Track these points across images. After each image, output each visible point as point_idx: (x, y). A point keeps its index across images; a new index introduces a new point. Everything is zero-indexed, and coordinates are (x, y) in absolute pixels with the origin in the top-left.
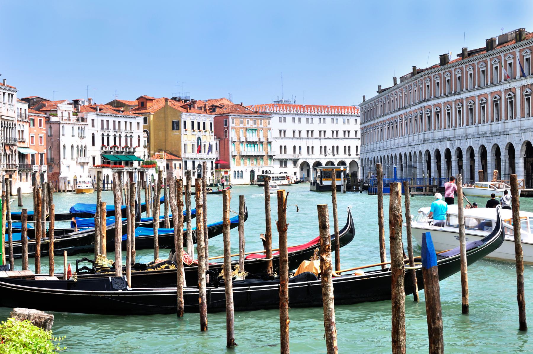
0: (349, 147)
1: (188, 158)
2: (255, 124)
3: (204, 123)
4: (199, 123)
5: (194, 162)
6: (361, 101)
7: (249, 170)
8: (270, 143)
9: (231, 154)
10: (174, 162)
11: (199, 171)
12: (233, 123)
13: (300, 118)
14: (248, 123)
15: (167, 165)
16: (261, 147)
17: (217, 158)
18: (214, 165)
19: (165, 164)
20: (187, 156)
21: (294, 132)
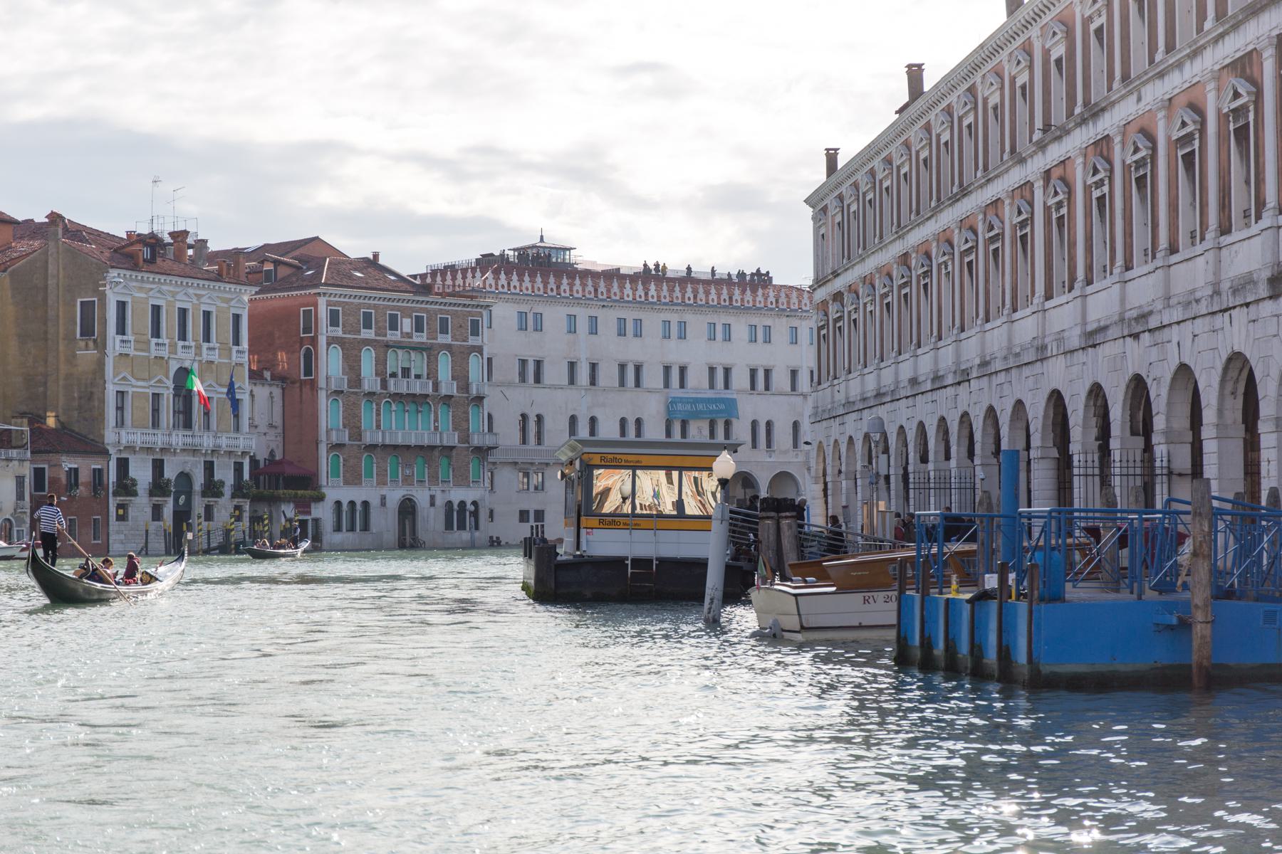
0: (769, 424)
1: (131, 448)
2: (419, 328)
3: (207, 315)
4: (183, 312)
5: (158, 466)
6: (820, 176)
7: (395, 495)
8: (479, 399)
9: (323, 436)
10: (68, 463)
11: (182, 500)
12: (334, 321)
13: (593, 321)
14: (394, 326)
15: (39, 474)
16: (441, 410)
17: (272, 453)
18: (246, 476)
19: (27, 470)
20: (126, 437)
21: (572, 365)
